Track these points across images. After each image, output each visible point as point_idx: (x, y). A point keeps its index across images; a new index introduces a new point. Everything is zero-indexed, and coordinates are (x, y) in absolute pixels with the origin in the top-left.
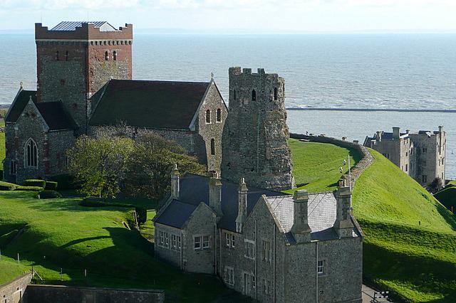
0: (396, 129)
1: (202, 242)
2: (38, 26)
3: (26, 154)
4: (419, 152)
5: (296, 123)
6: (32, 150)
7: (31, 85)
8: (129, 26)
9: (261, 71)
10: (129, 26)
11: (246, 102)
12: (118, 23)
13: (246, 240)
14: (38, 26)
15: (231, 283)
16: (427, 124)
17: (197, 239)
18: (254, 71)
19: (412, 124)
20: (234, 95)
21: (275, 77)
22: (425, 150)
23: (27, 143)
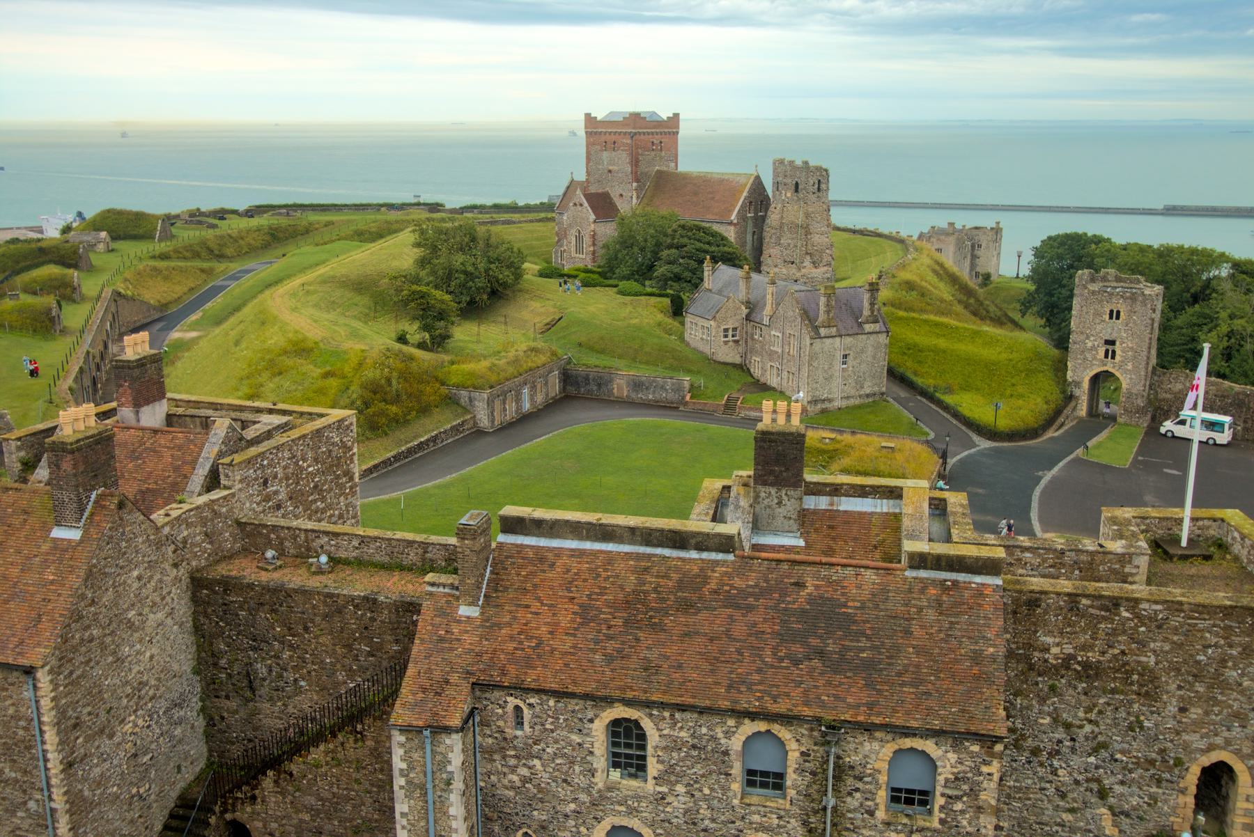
0: (951, 224)
1: (730, 333)
2: (588, 116)
3: (574, 242)
4: (973, 246)
5: (840, 217)
6: (579, 238)
7: (581, 176)
8: (676, 116)
9: (806, 163)
10: (676, 116)
11: (789, 195)
12: (665, 114)
13: (773, 333)
14: (588, 116)
15: (757, 372)
16: (986, 220)
17: (726, 330)
18: (799, 163)
19: (965, 220)
20: (777, 185)
21: (819, 169)
22: (980, 246)
23: (574, 232)
